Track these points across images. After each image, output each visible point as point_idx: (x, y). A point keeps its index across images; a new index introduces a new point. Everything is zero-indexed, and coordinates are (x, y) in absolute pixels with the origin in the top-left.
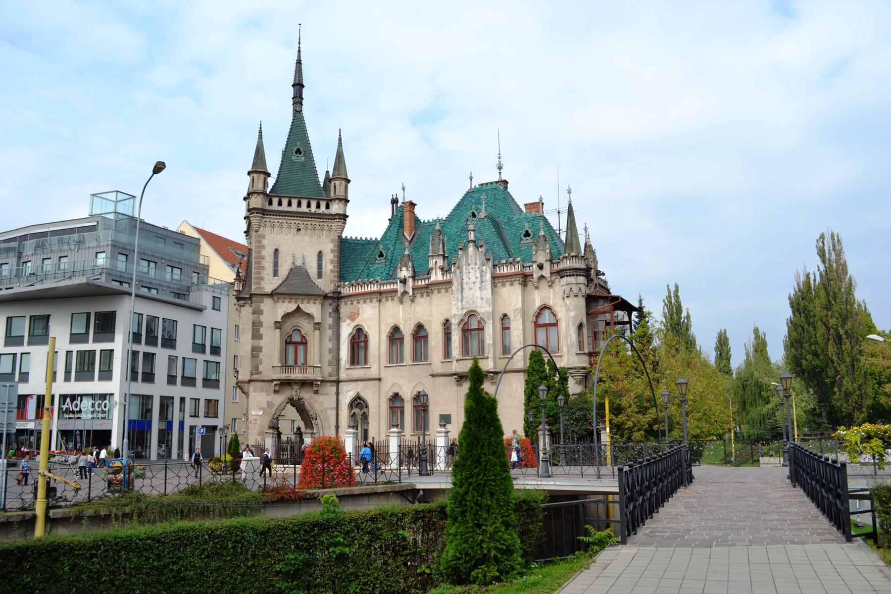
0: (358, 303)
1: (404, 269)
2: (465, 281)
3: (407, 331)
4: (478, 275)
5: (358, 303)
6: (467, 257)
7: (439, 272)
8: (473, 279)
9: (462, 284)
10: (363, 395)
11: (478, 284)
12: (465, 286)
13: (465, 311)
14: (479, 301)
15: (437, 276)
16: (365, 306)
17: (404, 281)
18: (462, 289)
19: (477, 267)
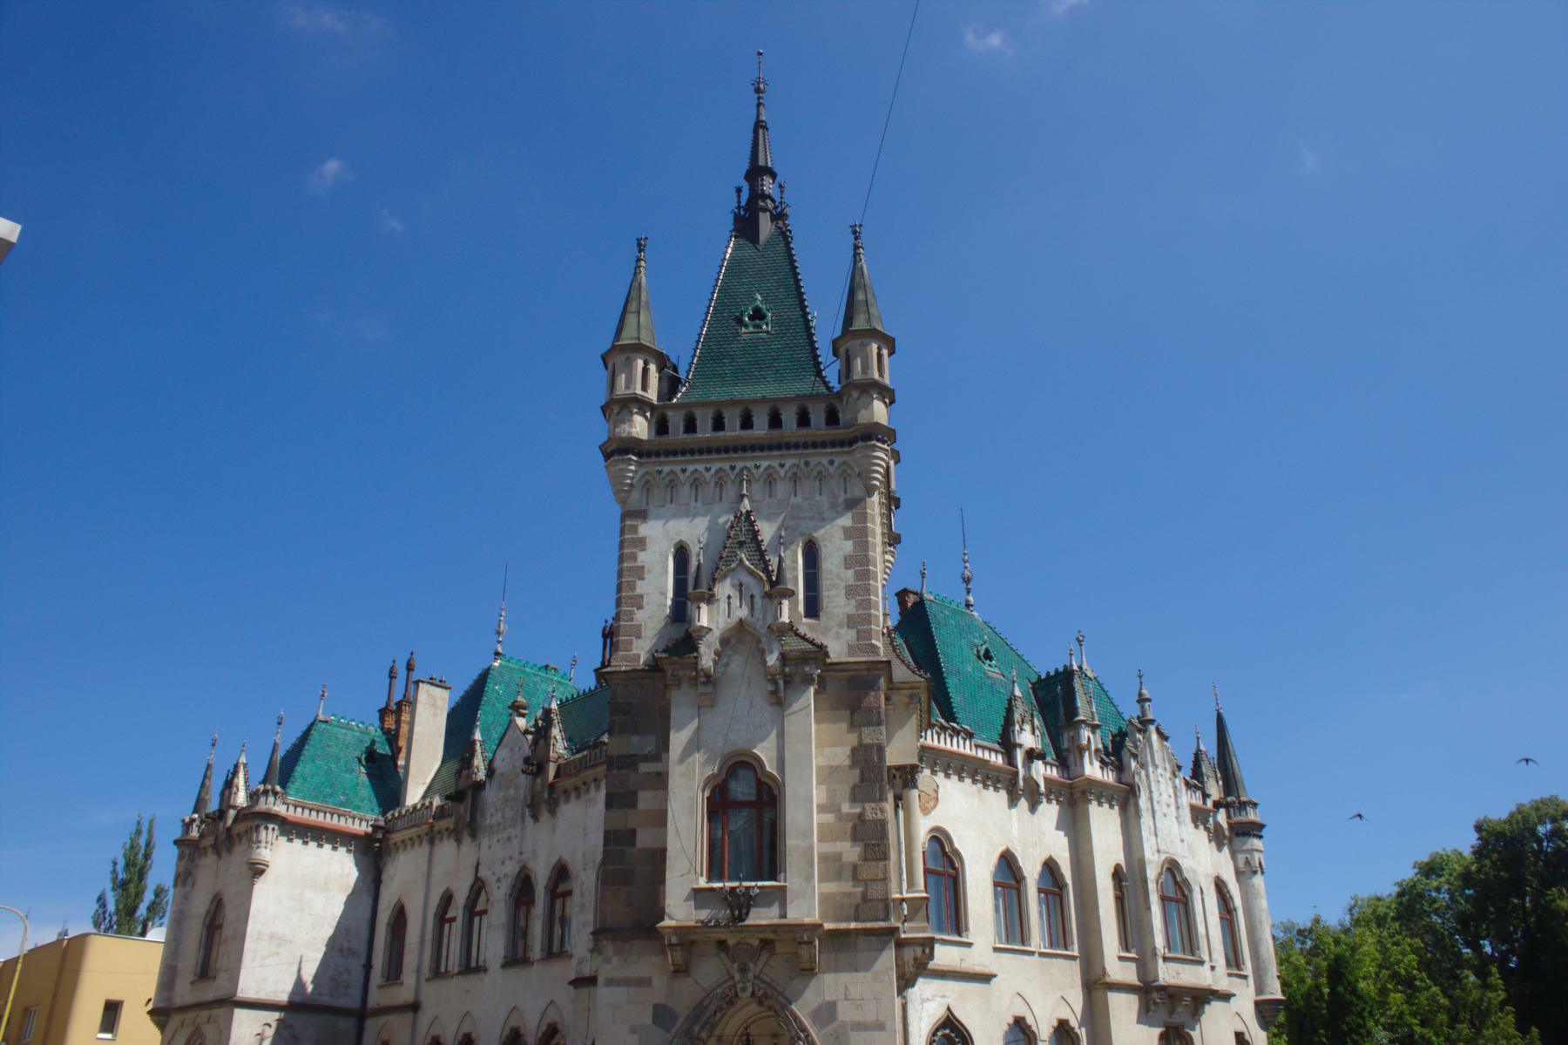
0: (934, 772)
1: (1027, 727)
2: (1155, 795)
3: (1031, 870)
4: (1171, 791)
5: (934, 772)
6: (1151, 747)
7: (1097, 764)
8: (1165, 796)
9: (1151, 799)
10: (959, 1014)
11: (1173, 808)
12: (1156, 806)
13: (1163, 857)
14: (1178, 842)
15: (1092, 769)
16: (947, 782)
17: (1031, 755)
18: (1154, 812)
19: (1168, 774)
